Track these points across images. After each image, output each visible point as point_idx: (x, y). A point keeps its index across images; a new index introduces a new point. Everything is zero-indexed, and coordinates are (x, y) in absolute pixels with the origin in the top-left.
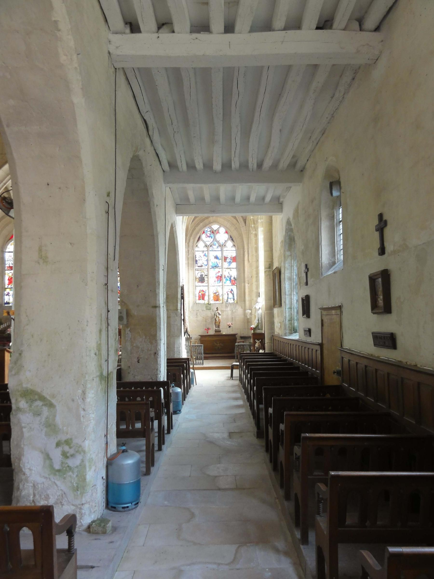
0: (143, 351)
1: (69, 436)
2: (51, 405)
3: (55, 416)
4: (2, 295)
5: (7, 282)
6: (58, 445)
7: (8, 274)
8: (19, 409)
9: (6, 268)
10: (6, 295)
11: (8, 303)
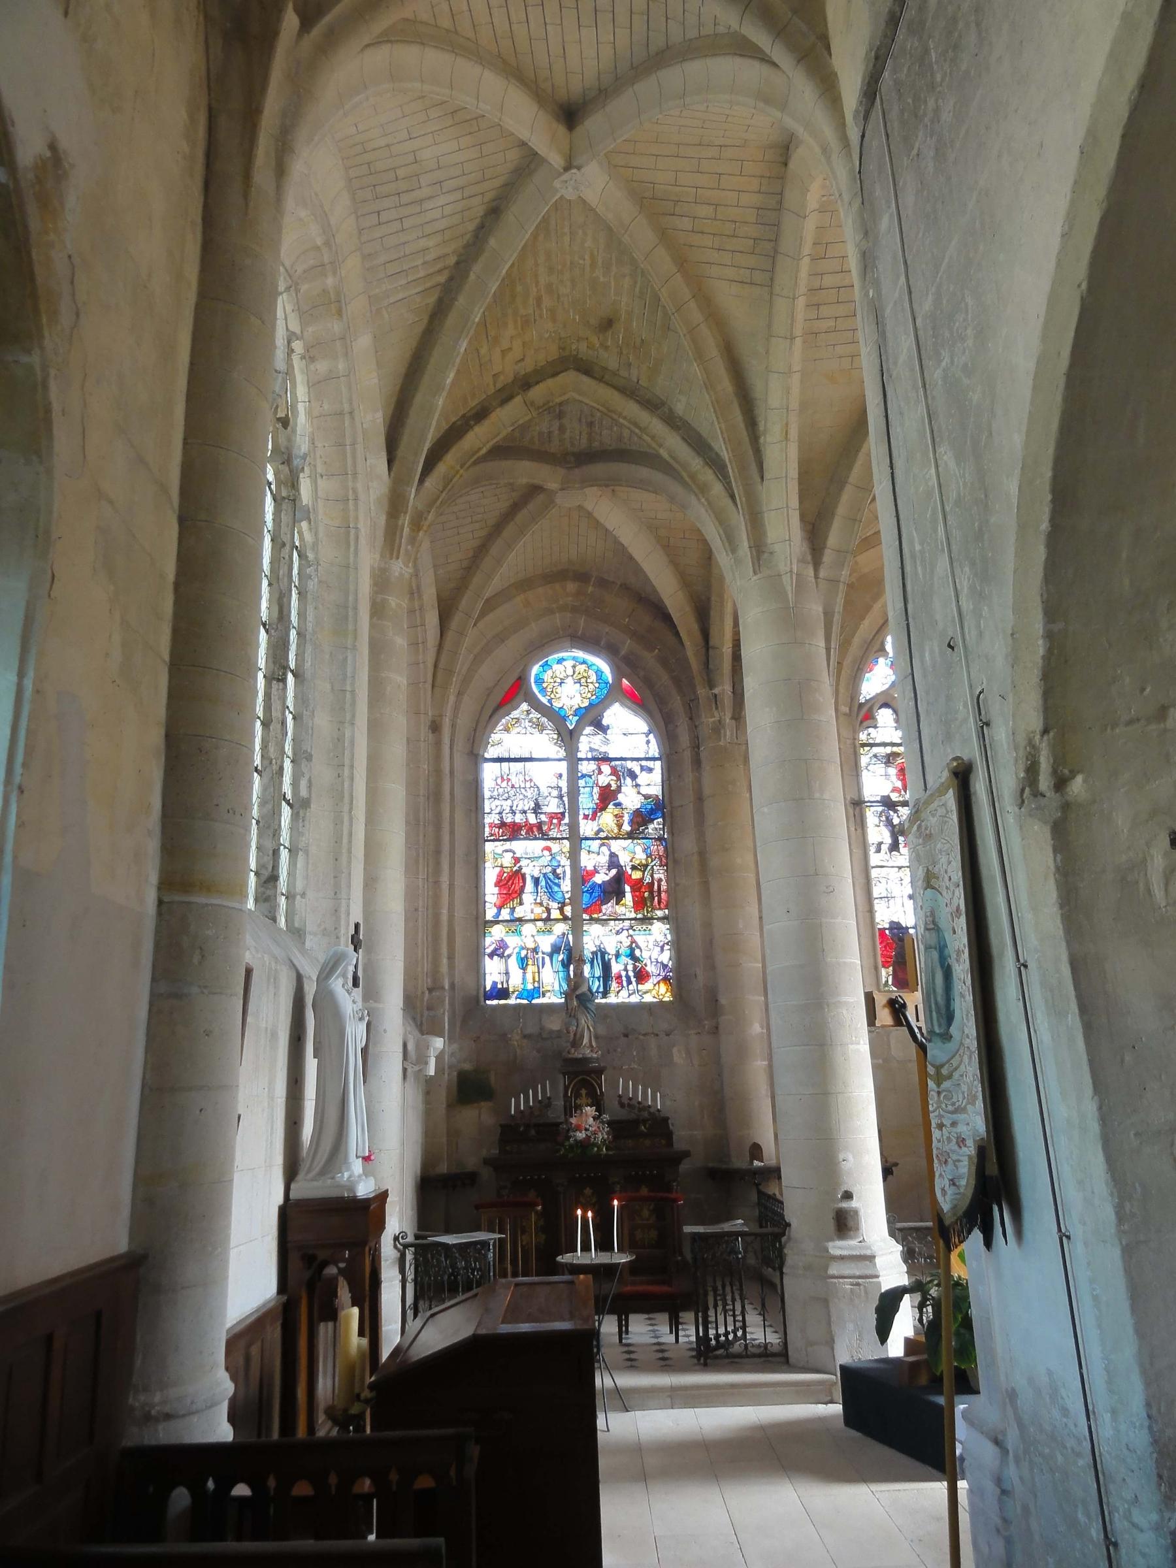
5: (491, 893)
9: (487, 830)
10: (491, 956)
11: (504, 993)
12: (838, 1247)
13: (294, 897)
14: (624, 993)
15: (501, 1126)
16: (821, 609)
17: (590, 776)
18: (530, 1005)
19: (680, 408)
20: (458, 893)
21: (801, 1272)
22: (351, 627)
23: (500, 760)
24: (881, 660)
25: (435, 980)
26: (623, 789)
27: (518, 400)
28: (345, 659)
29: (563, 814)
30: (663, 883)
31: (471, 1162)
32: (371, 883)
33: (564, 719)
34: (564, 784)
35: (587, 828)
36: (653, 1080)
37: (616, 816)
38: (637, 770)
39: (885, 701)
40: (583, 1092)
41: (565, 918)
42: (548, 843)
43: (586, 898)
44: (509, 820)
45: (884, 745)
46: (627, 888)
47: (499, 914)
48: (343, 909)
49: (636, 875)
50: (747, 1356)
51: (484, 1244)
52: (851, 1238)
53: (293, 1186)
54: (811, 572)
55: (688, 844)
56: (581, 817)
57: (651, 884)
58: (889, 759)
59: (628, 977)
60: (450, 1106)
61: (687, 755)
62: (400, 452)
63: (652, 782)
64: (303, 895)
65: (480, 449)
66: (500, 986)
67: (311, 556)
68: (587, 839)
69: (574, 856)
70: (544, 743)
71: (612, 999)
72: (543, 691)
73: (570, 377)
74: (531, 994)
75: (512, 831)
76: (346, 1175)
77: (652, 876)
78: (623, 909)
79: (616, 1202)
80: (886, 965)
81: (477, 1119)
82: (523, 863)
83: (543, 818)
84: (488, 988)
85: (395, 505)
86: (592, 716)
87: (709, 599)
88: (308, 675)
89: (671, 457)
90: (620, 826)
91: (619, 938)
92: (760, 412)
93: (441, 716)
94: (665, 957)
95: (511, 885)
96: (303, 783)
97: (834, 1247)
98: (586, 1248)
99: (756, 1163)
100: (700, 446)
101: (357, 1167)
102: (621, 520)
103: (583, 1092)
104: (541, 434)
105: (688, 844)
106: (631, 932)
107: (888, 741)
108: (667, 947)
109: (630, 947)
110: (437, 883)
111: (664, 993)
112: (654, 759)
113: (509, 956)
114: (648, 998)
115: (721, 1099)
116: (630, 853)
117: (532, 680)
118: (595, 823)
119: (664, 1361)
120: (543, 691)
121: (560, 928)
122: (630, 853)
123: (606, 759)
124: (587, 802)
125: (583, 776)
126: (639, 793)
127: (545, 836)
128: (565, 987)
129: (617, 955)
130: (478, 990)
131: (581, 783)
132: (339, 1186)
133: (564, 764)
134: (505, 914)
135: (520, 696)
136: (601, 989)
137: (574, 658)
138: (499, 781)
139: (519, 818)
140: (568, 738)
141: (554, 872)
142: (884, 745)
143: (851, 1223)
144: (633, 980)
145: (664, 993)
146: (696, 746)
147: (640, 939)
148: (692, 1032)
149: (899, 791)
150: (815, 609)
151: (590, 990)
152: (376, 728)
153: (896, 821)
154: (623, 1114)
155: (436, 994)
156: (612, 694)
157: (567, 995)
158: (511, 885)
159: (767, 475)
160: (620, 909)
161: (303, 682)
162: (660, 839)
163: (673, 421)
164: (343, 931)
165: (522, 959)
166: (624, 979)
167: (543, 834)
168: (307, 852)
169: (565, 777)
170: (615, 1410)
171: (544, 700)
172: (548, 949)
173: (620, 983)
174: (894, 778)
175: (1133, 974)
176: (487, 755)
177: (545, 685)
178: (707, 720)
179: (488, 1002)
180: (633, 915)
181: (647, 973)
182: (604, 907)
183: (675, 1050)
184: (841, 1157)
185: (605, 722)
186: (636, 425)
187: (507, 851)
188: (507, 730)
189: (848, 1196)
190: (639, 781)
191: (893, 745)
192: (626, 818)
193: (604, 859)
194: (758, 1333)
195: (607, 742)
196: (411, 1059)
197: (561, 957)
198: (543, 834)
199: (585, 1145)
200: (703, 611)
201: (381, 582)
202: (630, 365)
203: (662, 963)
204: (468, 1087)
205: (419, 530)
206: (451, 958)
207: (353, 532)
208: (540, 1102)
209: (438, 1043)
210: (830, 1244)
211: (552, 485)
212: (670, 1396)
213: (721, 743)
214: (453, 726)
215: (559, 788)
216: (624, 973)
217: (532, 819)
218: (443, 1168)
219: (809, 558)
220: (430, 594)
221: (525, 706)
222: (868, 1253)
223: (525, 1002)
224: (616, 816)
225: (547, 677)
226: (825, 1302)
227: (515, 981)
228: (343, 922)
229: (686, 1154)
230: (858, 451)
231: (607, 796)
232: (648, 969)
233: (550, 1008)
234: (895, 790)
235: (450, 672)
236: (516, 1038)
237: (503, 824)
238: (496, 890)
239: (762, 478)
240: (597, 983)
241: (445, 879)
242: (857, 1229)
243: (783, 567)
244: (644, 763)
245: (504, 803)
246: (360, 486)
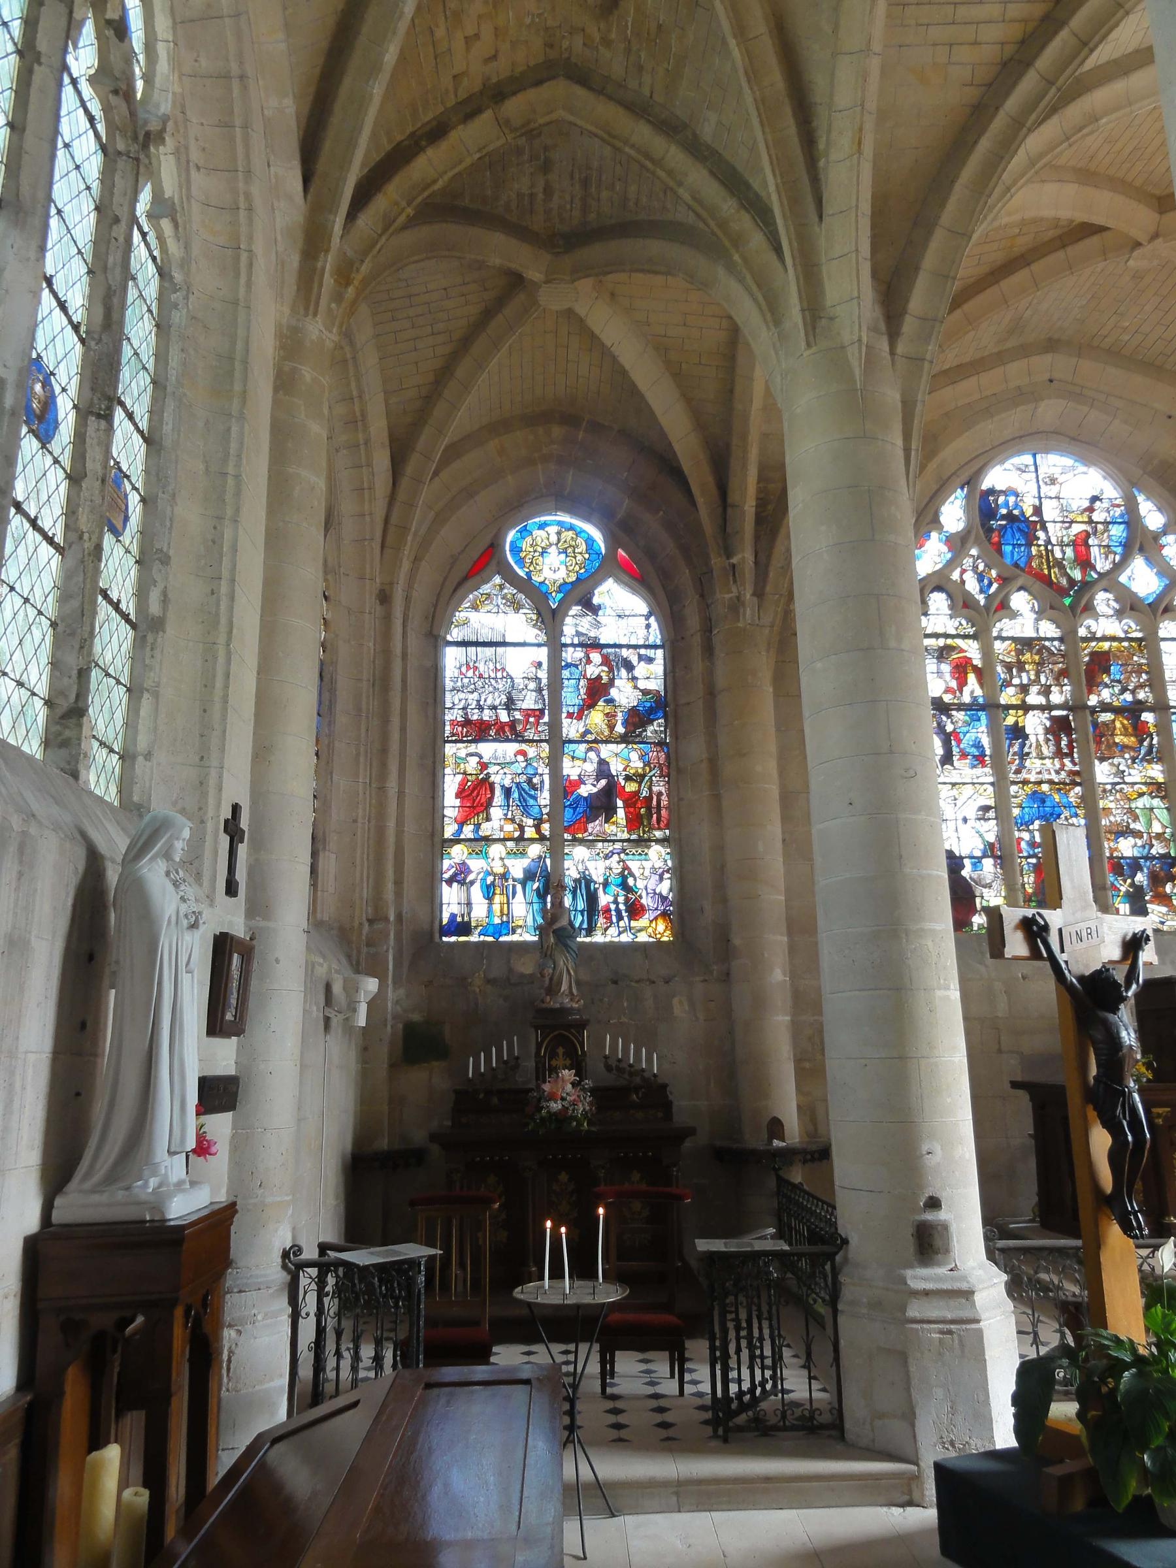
4: (431, 883)
7: (458, 761)
9: (448, 728)
10: (450, 882)
11: (464, 928)
12: (920, 1277)
13: (133, 757)
14: (613, 931)
15: (456, 1092)
16: (898, 397)
17: (576, 666)
18: (497, 944)
19: (707, 132)
20: (408, 802)
21: (864, 1311)
22: (237, 387)
23: (464, 644)
24: (934, 535)
25: (376, 909)
26: (617, 682)
27: (487, 115)
28: (229, 429)
29: (542, 711)
30: (664, 797)
31: (419, 1137)
32: (262, 753)
33: (546, 596)
34: (543, 675)
35: (571, 729)
36: (647, 1037)
37: (607, 715)
38: (634, 660)
39: (939, 582)
40: (561, 1051)
41: (542, 838)
42: (524, 746)
43: (568, 813)
44: (475, 717)
45: (936, 636)
46: (620, 803)
47: (460, 831)
48: (212, 781)
49: (631, 787)
50: (785, 1429)
51: (413, 1263)
52: (939, 1264)
53: (58, 1202)
54: (884, 345)
55: (696, 749)
56: (564, 715)
57: (649, 799)
58: (942, 654)
59: (618, 911)
60: (393, 1066)
61: (697, 640)
62: (322, 166)
63: (652, 675)
64: (148, 756)
65: (435, 182)
66: (459, 919)
67: (178, 276)
68: (571, 742)
69: (554, 762)
70: (518, 625)
71: (598, 938)
72: (521, 562)
73: (559, 89)
74: (498, 930)
75: (479, 731)
76: (153, 1182)
77: (650, 789)
78: (613, 828)
79: (601, 1211)
81: (428, 1081)
82: (492, 769)
83: (518, 715)
84: (445, 921)
85: (313, 241)
86: (580, 594)
87: (728, 446)
88: (168, 443)
89: (694, 198)
90: (611, 727)
91: (608, 862)
92: (820, 123)
93: (391, 584)
94: (665, 887)
95: (477, 796)
96: (154, 596)
97: (915, 1277)
98: (556, 1274)
99: (776, 1143)
100: (734, 183)
101: (175, 1169)
102: (622, 327)
103: (561, 1051)
104: (520, 195)
105: (696, 749)
106: (622, 855)
107: (941, 631)
108: (667, 876)
109: (622, 874)
110: (382, 789)
111: (662, 931)
112: (655, 647)
113: (472, 883)
114: (643, 938)
115: (731, 1060)
116: (624, 760)
117: (507, 548)
118: (582, 723)
119: (667, 1436)
120: (521, 562)
121: (535, 850)
122: (624, 760)
123: (595, 645)
124: (571, 697)
125: (568, 665)
126: (636, 687)
127: (519, 738)
128: (540, 921)
129: (606, 884)
130: (432, 922)
131: (566, 673)
132: (139, 1203)
133: (545, 650)
134: (468, 831)
135: (493, 565)
136: (585, 926)
137: (560, 523)
138: (464, 669)
139: (487, 715)
140: (549, 620)
141: (529, 781)
142: (936, 636)
143: (938, 1243)
144: (624, 914)
145: (662, 931)
146: (708, 629)
147: (634, 865)
148: (698, 979)
149: (954, 692)
150: (892, 395)
151: (571, 924)
152: (276, 541)
153: (949, 728)
154: (610, 1079)
155: (379, 926)
156: (604, 567)
157: (541, 930)
158: (477, 796)
159: (828, 210)
160: (610, 829)
161: (159, 452)
162: (661, 744)
163: (697, 149)
164: (211, 813)
165: (488, 887)
166: (613, 913)
167: (517, 735)
168: (156, 695)
169: (545, 666)
170: (596, 1512)
171: (521, 573)
172: (519, 874)
173: (609, 919)
174: (948, 677)
176: (449, 638)
177: (523, 555)
178: (723, 596)
179: (445, 939)
180: (625, 836)
181: (642, 906)
182: (590, 826)
183: (675, 1001)
184: (925, 1148)
185: (596, 601)
186: (647, 156)
187: (471, 755)
188: (475, 608)
189: (934, 1203)
190: (636, 673)
191: (946, 636)
192: (620, 717)
193: (590, 767)
194: (797, 1384)
195: (597, 625)
196: (328, 1002)
197: (536, 885)
198: (517, 735)
199: (561, 1118)
200: (721, 462)
201: (290, 344)
202: (640, 68)
203: (660, 895)
204: (417, 1043)
205: (348, 284)
206: (398, 883)
207: (244, 256)
208: (505, 1062)
209: (371, 985)
210: (909, 1273)
211: (534, 274)
212: (677, 1494)
213: (740, 625)
214: (407, 599)
215: (537, 679)
216: (613, 907)
217: (504, 717)
218: (383, 1144)
219: (882, 326)
220: (378, 427)
221: (497, 580)
222: (964, 1286)
223: (491, 939)
224: (607, 715)
225: (525, 545)
226: (902, 1357)
227: (479, 911)
228: (211, 801)
229: (691, 1132)
230: (953, 182)
231: (597, 691)
232: (644, 901)
233: (522, 946)
234: (948, 690)
235: (404, 529)
236: (477, 982)
237: (467, 722)
238: (458, 802)
239: (821, 217)
240: (580, 918)
241: (392, 784)
242: (947, 1251)
243: (847, 336)
244: (643, 651)
245: (471, 696)
246: (255, 190)
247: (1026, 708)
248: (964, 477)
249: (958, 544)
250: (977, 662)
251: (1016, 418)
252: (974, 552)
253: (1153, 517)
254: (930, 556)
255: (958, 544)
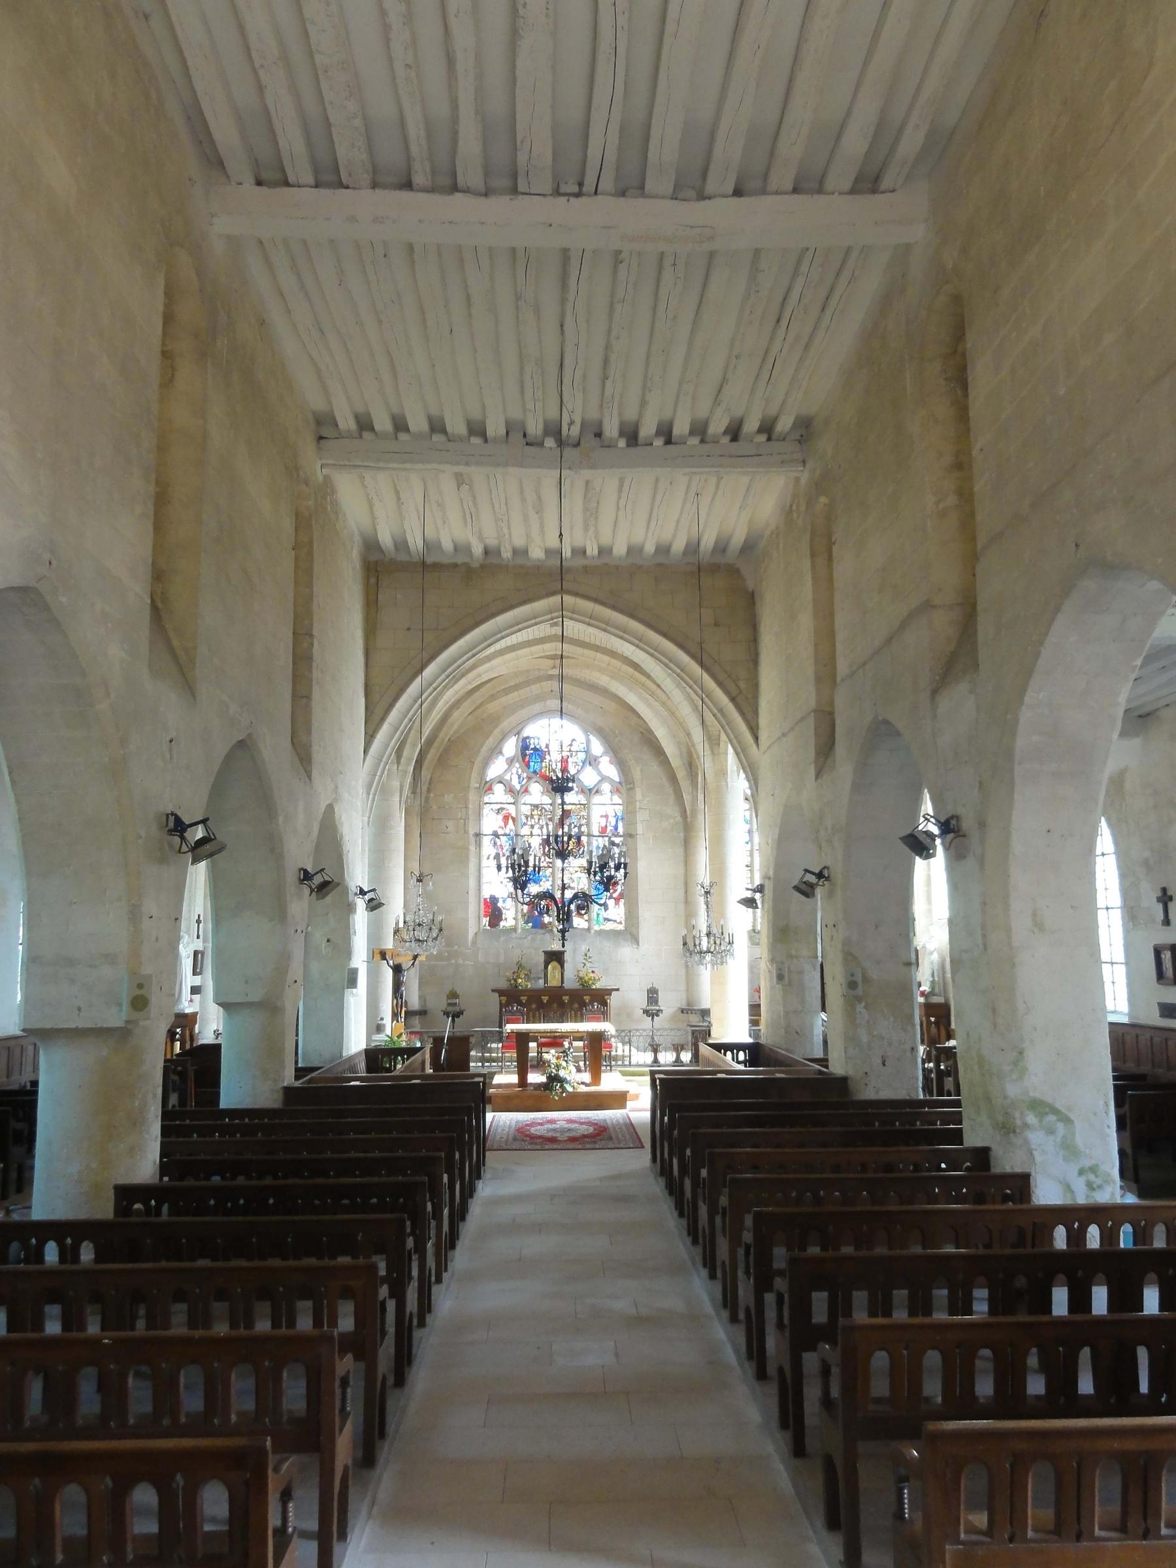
0: (890, 1044)
1: (1093, 1162)
2: (1067, 1120)
3: (1074, 1134)
6: (1081, 1172)
8: (1026, 1126)
80: (485, 916)
101: (186, 1004)
150: (396, 784)
175: (315, 967)
247: (532, 835)
248: (516, 731)
249: (510, 762)
250: (514, 815)
251: (537, 707)
252: (517, 765)
253: (597, 747)
254: (496, 768)
255: (510, 762)
